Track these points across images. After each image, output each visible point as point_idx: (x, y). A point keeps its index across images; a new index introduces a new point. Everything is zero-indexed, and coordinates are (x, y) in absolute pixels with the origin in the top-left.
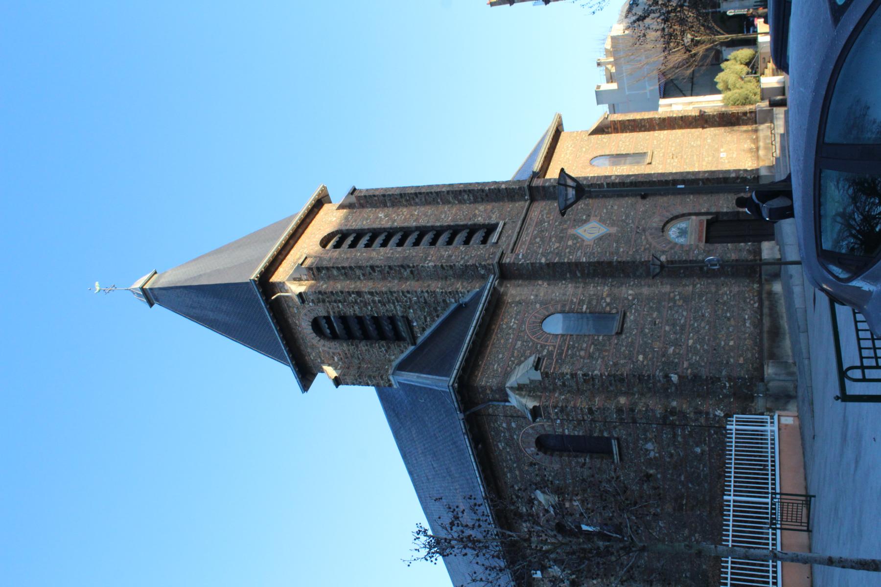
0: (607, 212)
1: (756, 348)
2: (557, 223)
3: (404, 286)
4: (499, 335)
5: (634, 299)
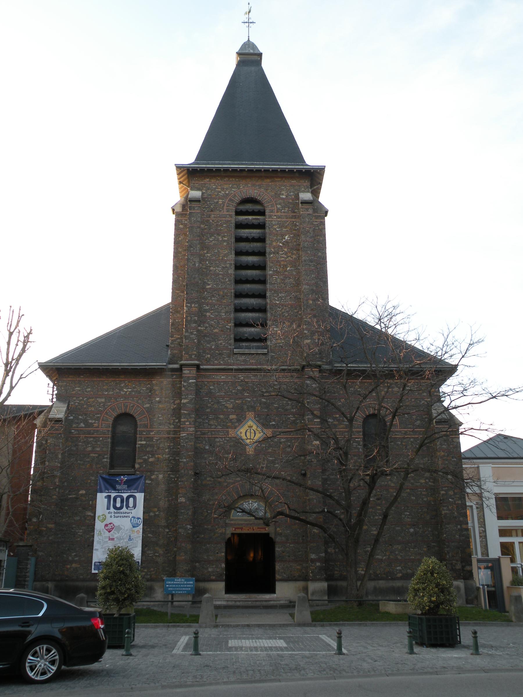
1: (89, 577)
2: (263, 400)
4: (112, 383)
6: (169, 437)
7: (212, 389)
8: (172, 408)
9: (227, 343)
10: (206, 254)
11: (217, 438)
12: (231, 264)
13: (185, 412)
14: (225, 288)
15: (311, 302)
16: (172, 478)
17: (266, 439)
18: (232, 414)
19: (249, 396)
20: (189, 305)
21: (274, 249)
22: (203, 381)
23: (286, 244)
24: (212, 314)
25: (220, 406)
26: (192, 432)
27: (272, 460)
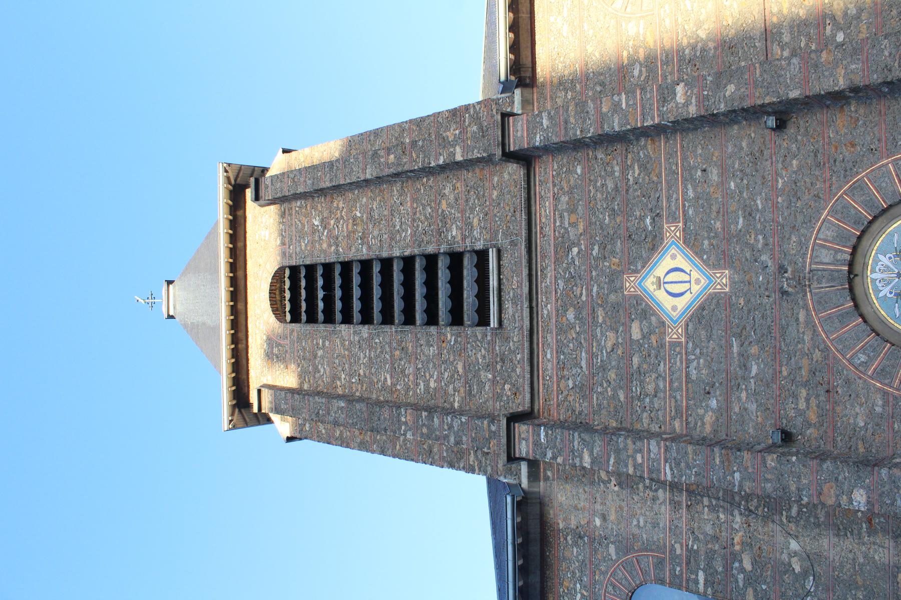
0: (697, 198)
3: (398, 447)
5: (805, 574)
6: (688, 506)
7: (574, 383)
8: (616, 488)
9: (481, 343)
10: (341, 383)
11: (687, 374)
12: (355, 333)
13: (612, 461)
14: (390, 344)
15: (392, 156)
16: (800, 512)
17: (691, 242)
18: (628, 330)
19: (587, 289)
20: (403, 427)
21: (331, 246)
22: (558, 406)
23: (324, 223)
24: (431, 376)
25: (610, 363)
26: (660, 448)
27: (744, 217)
